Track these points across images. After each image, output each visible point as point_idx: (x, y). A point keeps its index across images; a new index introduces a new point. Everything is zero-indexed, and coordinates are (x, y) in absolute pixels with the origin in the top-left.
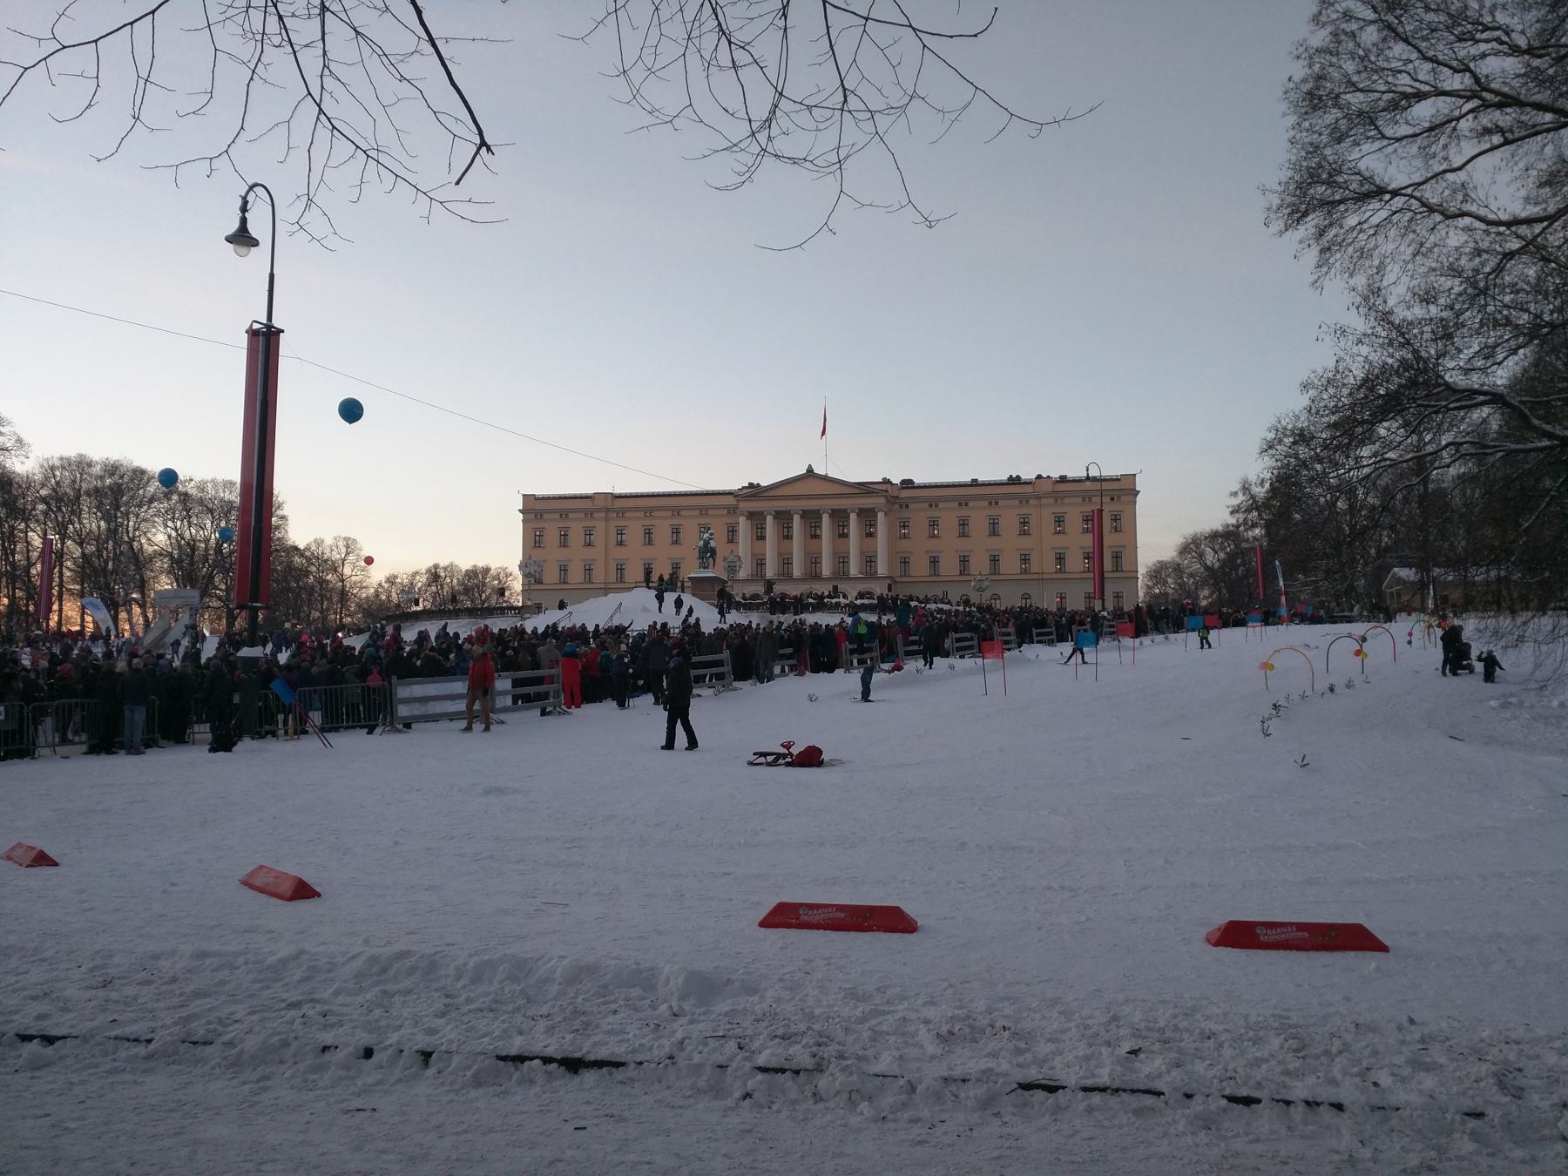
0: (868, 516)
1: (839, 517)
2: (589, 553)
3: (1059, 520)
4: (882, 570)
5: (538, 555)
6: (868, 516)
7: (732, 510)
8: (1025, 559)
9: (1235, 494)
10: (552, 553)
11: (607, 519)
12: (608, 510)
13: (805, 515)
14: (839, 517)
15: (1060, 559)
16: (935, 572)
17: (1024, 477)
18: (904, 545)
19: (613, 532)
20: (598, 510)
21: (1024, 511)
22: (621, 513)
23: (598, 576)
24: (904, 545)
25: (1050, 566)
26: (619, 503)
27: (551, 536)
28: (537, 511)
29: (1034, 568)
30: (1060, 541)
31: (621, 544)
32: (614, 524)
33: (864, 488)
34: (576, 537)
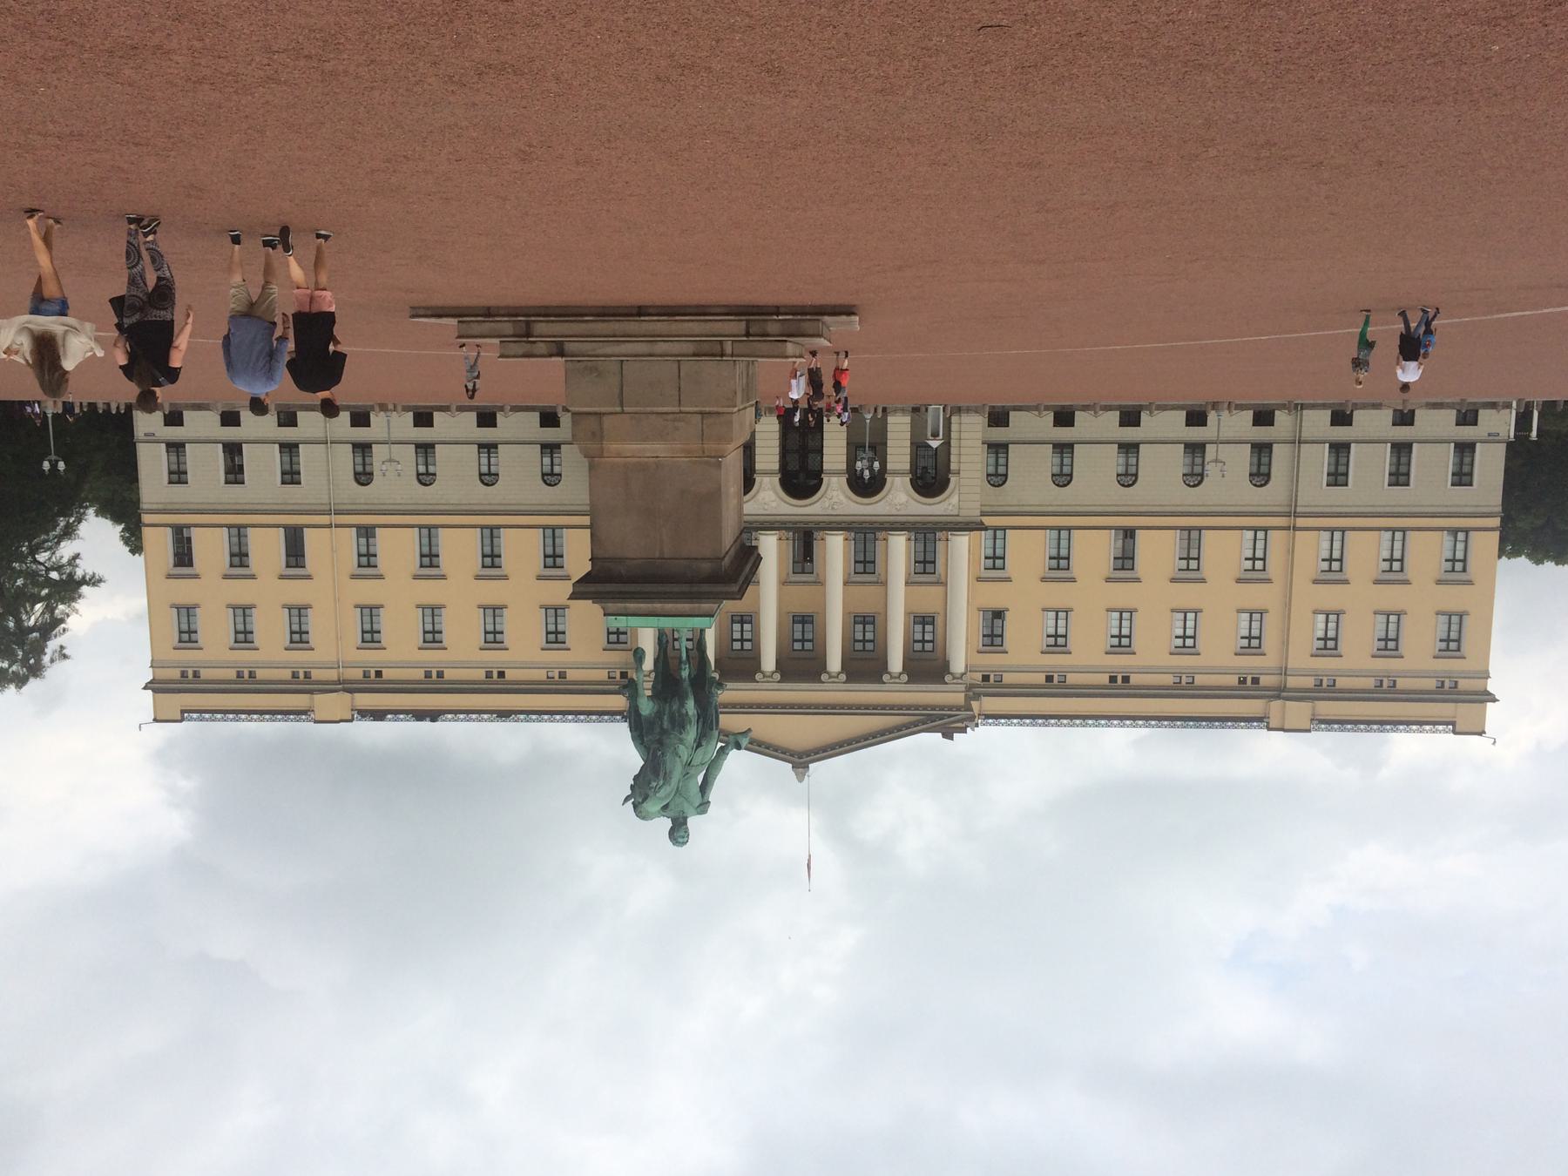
3: (299, 637)
7: (990, 684)
8: (367, 559)
10: (1422, 602)
11: (1284, 671)
12: (1280, 693)
19: (1271, 642)
20: (1302, 695)
21: (372, 657)
22: (1248, 686)
23: (1312, 547)
28: (1456, 698)
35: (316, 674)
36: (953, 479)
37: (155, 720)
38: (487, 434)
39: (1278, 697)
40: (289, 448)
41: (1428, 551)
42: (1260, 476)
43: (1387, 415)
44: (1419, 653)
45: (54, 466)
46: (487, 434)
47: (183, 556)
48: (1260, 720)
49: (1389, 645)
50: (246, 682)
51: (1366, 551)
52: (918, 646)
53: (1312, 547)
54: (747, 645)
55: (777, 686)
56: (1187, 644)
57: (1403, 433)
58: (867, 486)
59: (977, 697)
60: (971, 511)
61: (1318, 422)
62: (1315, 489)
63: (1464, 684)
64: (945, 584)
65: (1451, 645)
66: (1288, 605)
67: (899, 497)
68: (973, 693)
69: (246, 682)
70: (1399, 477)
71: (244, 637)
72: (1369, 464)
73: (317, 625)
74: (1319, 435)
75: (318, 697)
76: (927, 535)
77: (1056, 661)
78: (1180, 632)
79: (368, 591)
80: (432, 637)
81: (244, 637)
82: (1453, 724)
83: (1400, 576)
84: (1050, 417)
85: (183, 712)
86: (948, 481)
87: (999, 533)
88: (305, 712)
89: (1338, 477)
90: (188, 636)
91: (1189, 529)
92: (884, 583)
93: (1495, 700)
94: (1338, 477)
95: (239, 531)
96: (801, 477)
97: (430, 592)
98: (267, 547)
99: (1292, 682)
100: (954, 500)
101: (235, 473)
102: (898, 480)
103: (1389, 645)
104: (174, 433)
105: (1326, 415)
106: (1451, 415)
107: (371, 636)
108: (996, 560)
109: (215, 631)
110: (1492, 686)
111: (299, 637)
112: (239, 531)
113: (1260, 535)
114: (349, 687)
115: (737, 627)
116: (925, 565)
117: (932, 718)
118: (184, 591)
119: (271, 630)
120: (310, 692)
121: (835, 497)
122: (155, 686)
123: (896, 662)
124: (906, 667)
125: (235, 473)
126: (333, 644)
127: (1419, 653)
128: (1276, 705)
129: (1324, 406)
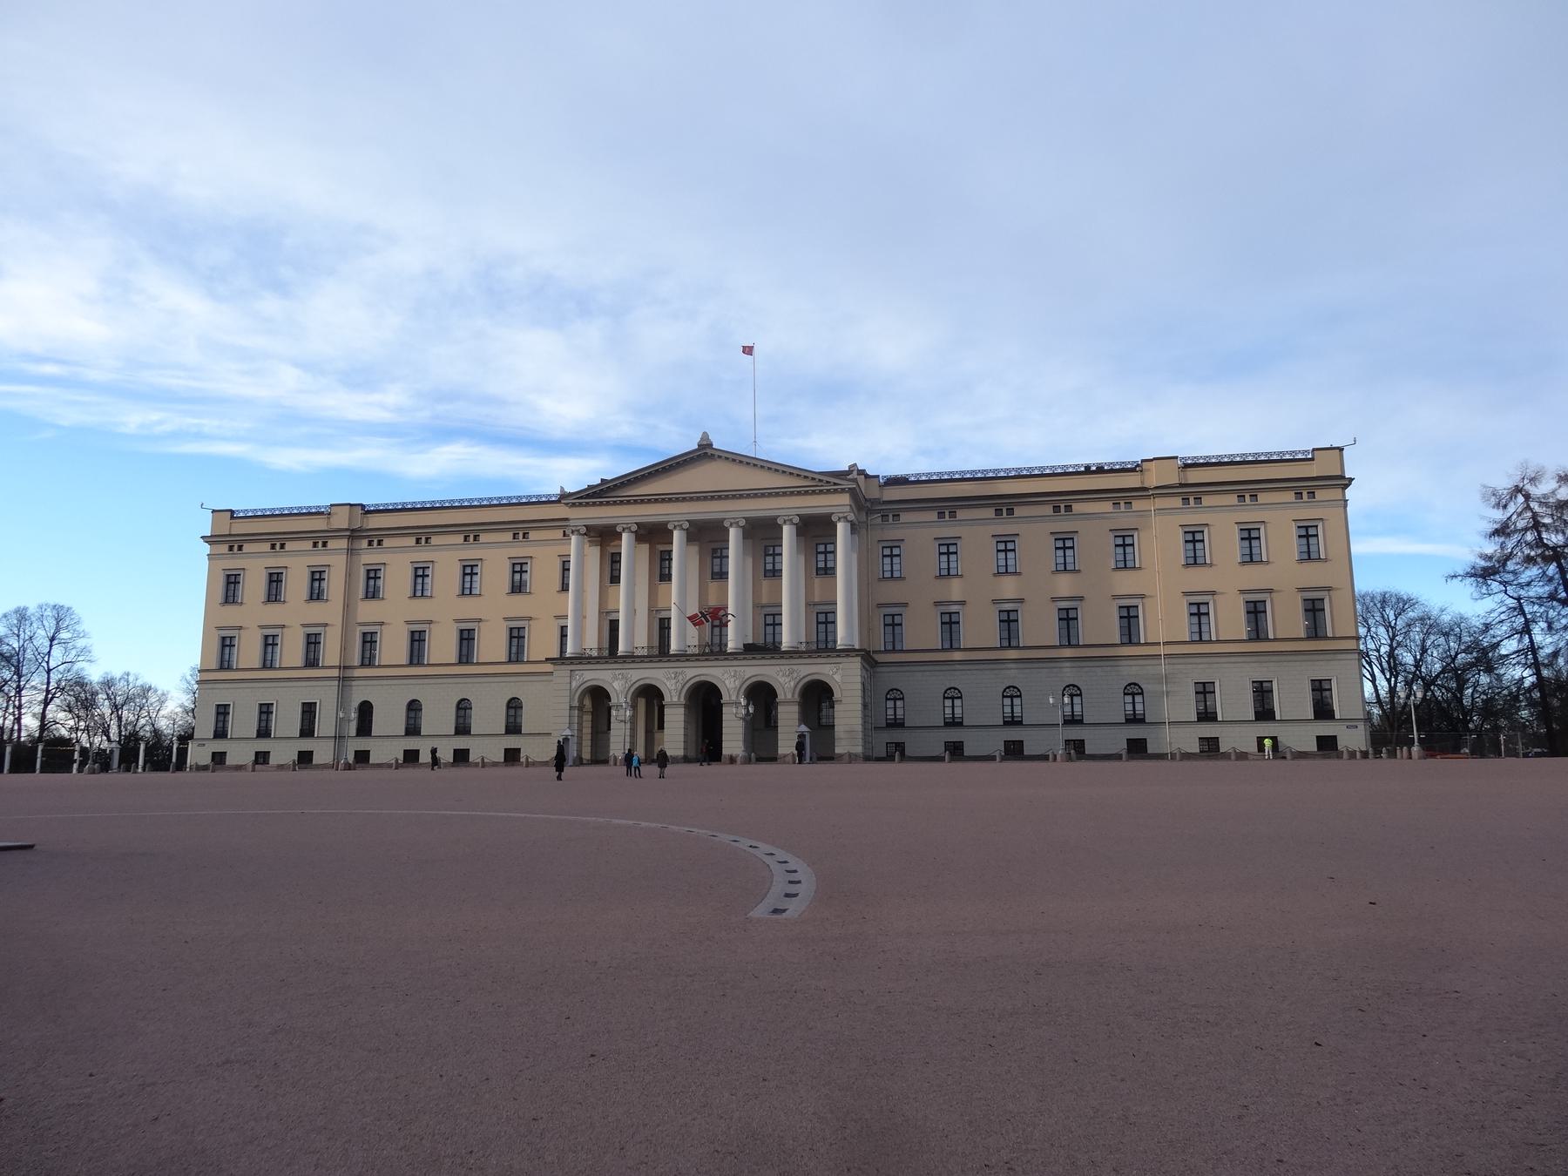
0: (816, 531)
1: (762, 534)
2: (316, 612)
3: (1193, 537)
4: (844, 633)
5: (232, 615)
6: (816, 531)
10: (253, 612)
11: (351, 552)
12: (354, 534)
14: (762, 534)
15: (1199, 613)
16: (951, 642)
20: (336, 533)
23: (330, 653)
24: (891, 592)
26: (375, 522)
27: (254, 586)
28: (232, 536)
30: (1198, 579)
31: (372, 594)
34: (296, 585)
37: (1341, 449)
38: (1014, 734)
40: (1207, 716)
41: (248, 652)
42: (366, 710)
43: (274, 760)
46: (1014, 734)
47: (1314, 609)
48: (369, 512)
50: (1247, 490)
57: (263, 745)
60: (562, 672)
61: (323, 752)
62: (326, 699)
63: (224, 548)
66: (348, 607)
69: (1247, 490)
70: (265, 710)
71: (1250, 535)
72: (287, 721)
74: (322, 743)
75: (1175, 480)
84: (472, 758)
88: (1187, 466)
89: (309, 710)
90: (1307, 533)
94: (309, 710)
95: (1258, 634)
96: (705, 700)
99: (343, 544)
101: (1262, 692)
104: (1325, 729)
105: (316, 760)
106: (230, 761)
109: (1280, 539)
110: (207, 548)
111: (1193, 537)
112: (1258, 634)
114: (1142, 492)
118: (1312, 575)
119: (1223, 541)
120: (1182, 485)
121: (673, 683)
122: (1344, 482)
125: (1262, 692)
129: (318, 767)
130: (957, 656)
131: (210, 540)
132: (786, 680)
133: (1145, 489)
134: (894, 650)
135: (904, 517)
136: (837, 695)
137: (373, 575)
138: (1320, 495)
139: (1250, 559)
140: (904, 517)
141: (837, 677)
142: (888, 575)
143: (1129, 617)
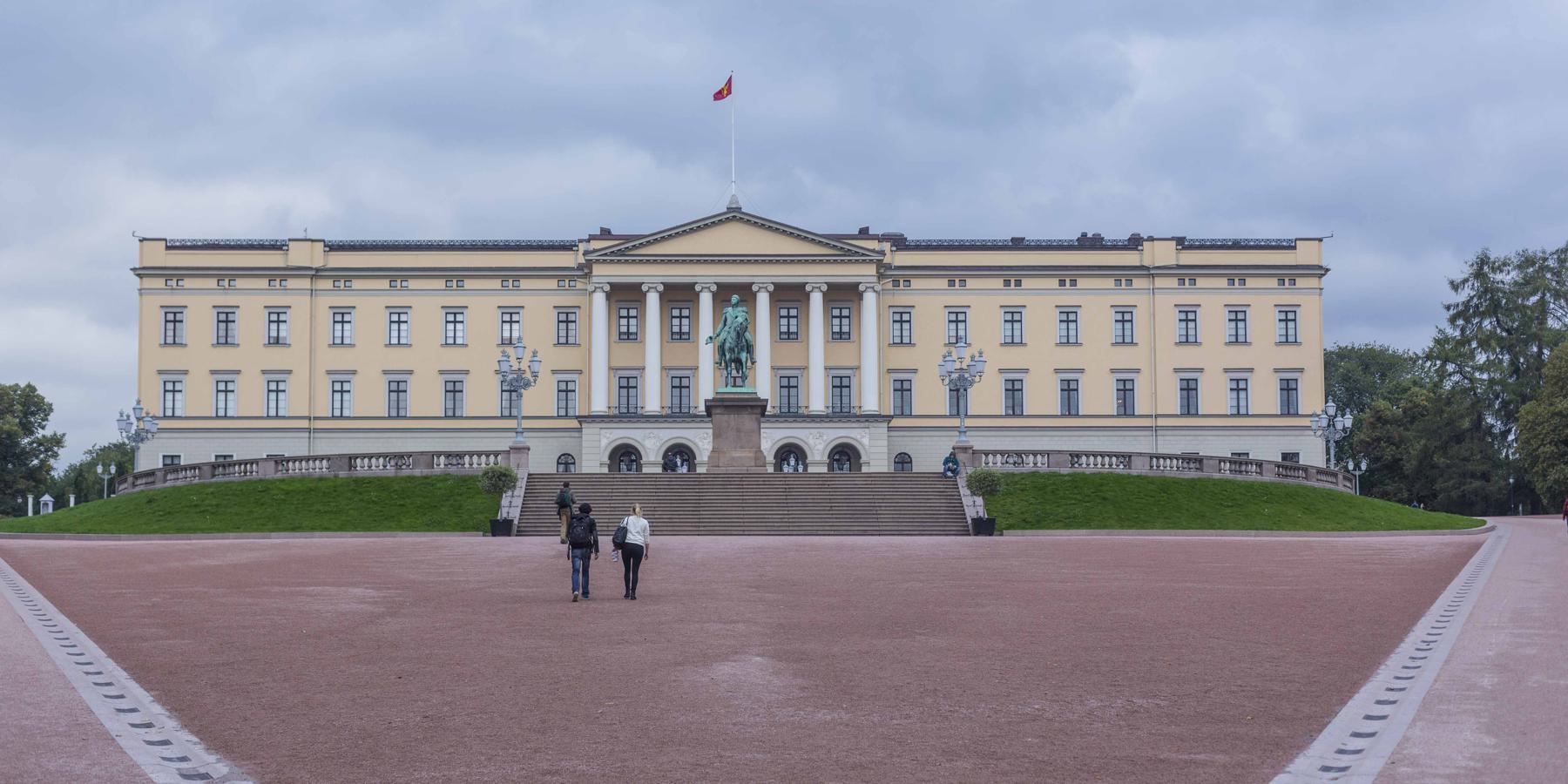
0: (843, 296)
2: (277, 359)
3: (1188, 316)
4: (871, 395)
5: (173, 359)
9: (1455, 286)
10: (199, 353)
12: (317, 273)
13: (723, 293)
15: (1189, 389)
17: (1109, 235)
18: (902, 358)
19: (325, 317)
21: (1124, 299)
22: (345, 276)
23: (294, 402)
24: (902, 358)
25: (1171, 401)
29: (1142, 405)
32: (326, 302)
33: (840, 247)
35: (1174, 282)
36: (606, 459)
37: (1320, 240)
39: (317, 270)
41: (197, 398)
44: (200, 306)
45: (1357, 466)
49: (225, 318)
50: (1237, 275)
51: (249, 399)
52: (633, 312)
53: (294, 402)
54: (784, 312)
55: (755, 280)
56: (398, 316)
58: (679, 454)
59: (580, 267)
60: (589, 431)
63: (160, 283)
64: (610, 368)
65: (173, 317)
67: (652, 444)
68: (585, 270)
71: (1238, 316)
73: (1171, 327)
76: (628, 414)
77: (511, 300)
78: (403, 326)
79: (1125, 358)
80: (1069, 316)
81: (1238, 316)
82: (168, 248)
83: (220, 377)
85: (1294, 248)
86: (610, 457)
87: (562, 413)
91: (454, 417)
92: (663, 368)
93: (134, 270)
97: (1069, 358)
98: (1214, 397)
99: (305, 283)
100: (604, 442)
102: (652, 458)
103: (225, 318)
107: (1124, 317)
108: (565, 391)
111: (1188, 316)
113: (337, 413)
115: (793, 329)
116: (628, 384)
117: (621, 253)
120: (1179, 267)
123: (653, 300)
124: (644, 294)
126: (1158, 308)
127: (200, 306)
128: (318, 264)
130: (969, 422)
131: (142, 272)
132: (818, 443)
133: (1147, 268)
134: (902, 415)
135: (915, 283)
136: (864, 458)
137: (341, 316)
138: (1300, 282)
139: (1237, 341)
140: (915, 283)
141: (866, 441)
142: (898, 340)
143: (1125, 390)
